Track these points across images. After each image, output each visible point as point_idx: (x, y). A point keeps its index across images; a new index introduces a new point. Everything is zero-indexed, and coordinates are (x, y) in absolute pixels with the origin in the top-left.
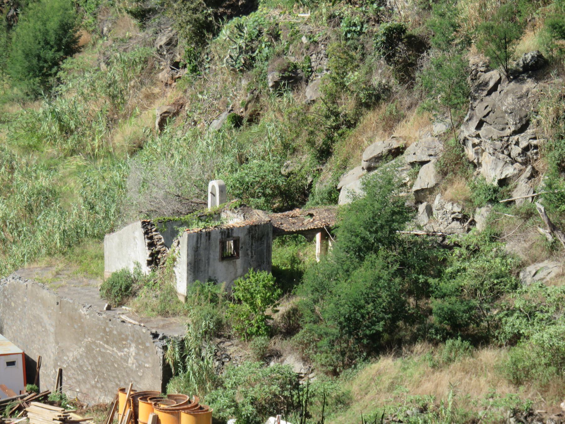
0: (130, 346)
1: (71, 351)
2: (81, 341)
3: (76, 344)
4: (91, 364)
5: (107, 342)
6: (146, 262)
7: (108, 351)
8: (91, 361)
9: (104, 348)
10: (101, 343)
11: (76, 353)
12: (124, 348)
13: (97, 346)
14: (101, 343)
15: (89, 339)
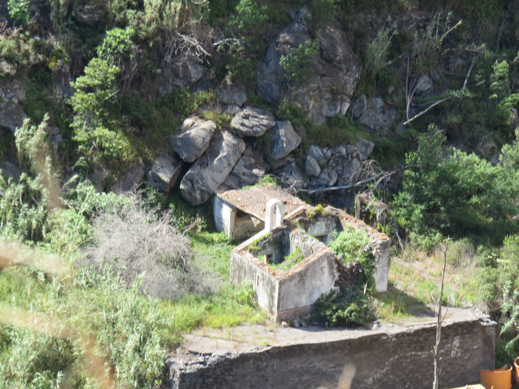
0: (453, 340)
1: (370, 376)
2: (384, 363)
3: (378, 368)
4: (399, 376)
5: (422, 349)
6: (334, 283)
7: (423, 356)
8: (400, 373)
9: (417, 355)
10: (413, 353)
11: (378, 376)
12: (445, 345)
13: (407, 358)
14: (413, 353)
15: (396, 357)
